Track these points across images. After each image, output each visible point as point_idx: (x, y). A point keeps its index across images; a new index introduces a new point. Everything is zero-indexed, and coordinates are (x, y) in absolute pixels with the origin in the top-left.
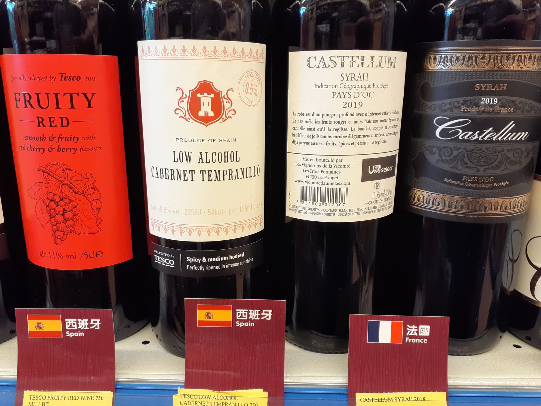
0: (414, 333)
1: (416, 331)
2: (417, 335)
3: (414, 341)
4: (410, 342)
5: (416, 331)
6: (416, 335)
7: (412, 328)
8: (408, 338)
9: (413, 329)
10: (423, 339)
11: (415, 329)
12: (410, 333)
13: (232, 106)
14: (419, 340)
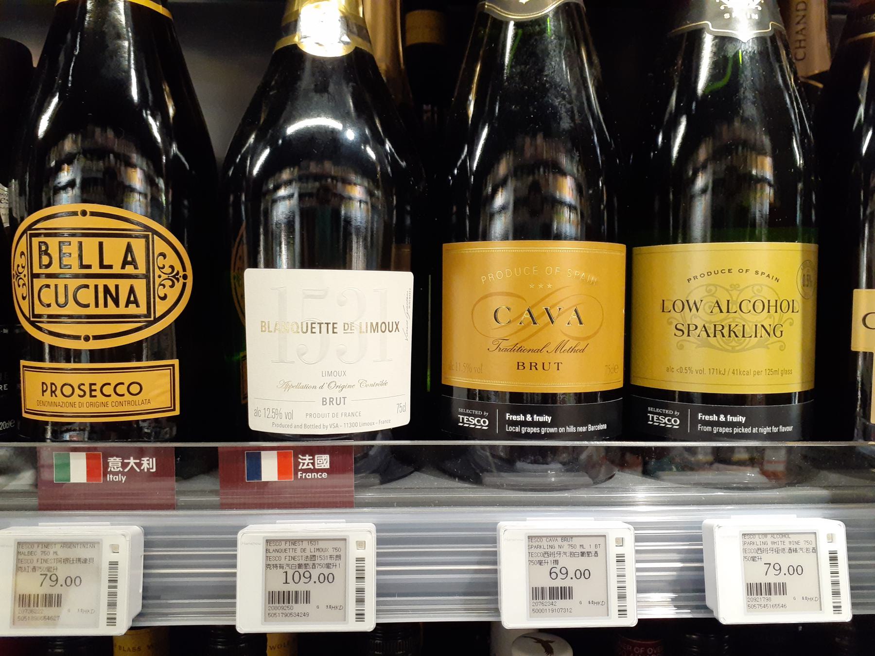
0: (308, 465)
1: (311, 463)
2: (312, 468)
3: (309, 476)
4: (304, 477)
5: (311, 463)
6: (310, 468)
7: (305, 459)
8: (301, 473)
9: (307, 459)
10: (321, 474)
11: (309, 459)
12: (303, 466)
13: (138, 396)
14: (316, 474)
